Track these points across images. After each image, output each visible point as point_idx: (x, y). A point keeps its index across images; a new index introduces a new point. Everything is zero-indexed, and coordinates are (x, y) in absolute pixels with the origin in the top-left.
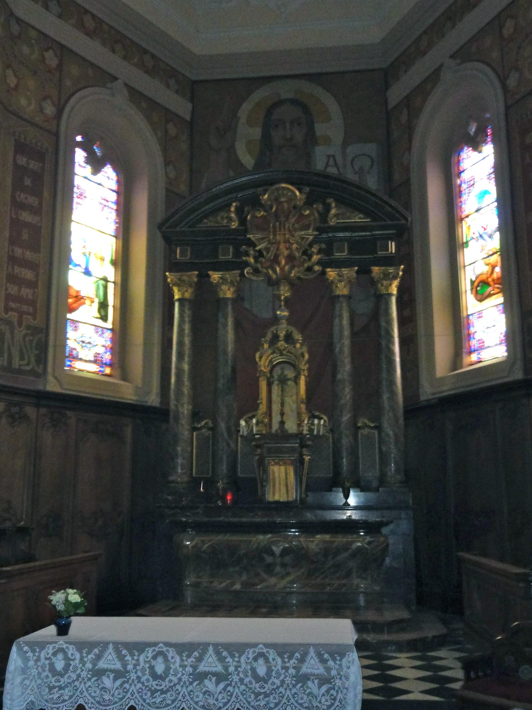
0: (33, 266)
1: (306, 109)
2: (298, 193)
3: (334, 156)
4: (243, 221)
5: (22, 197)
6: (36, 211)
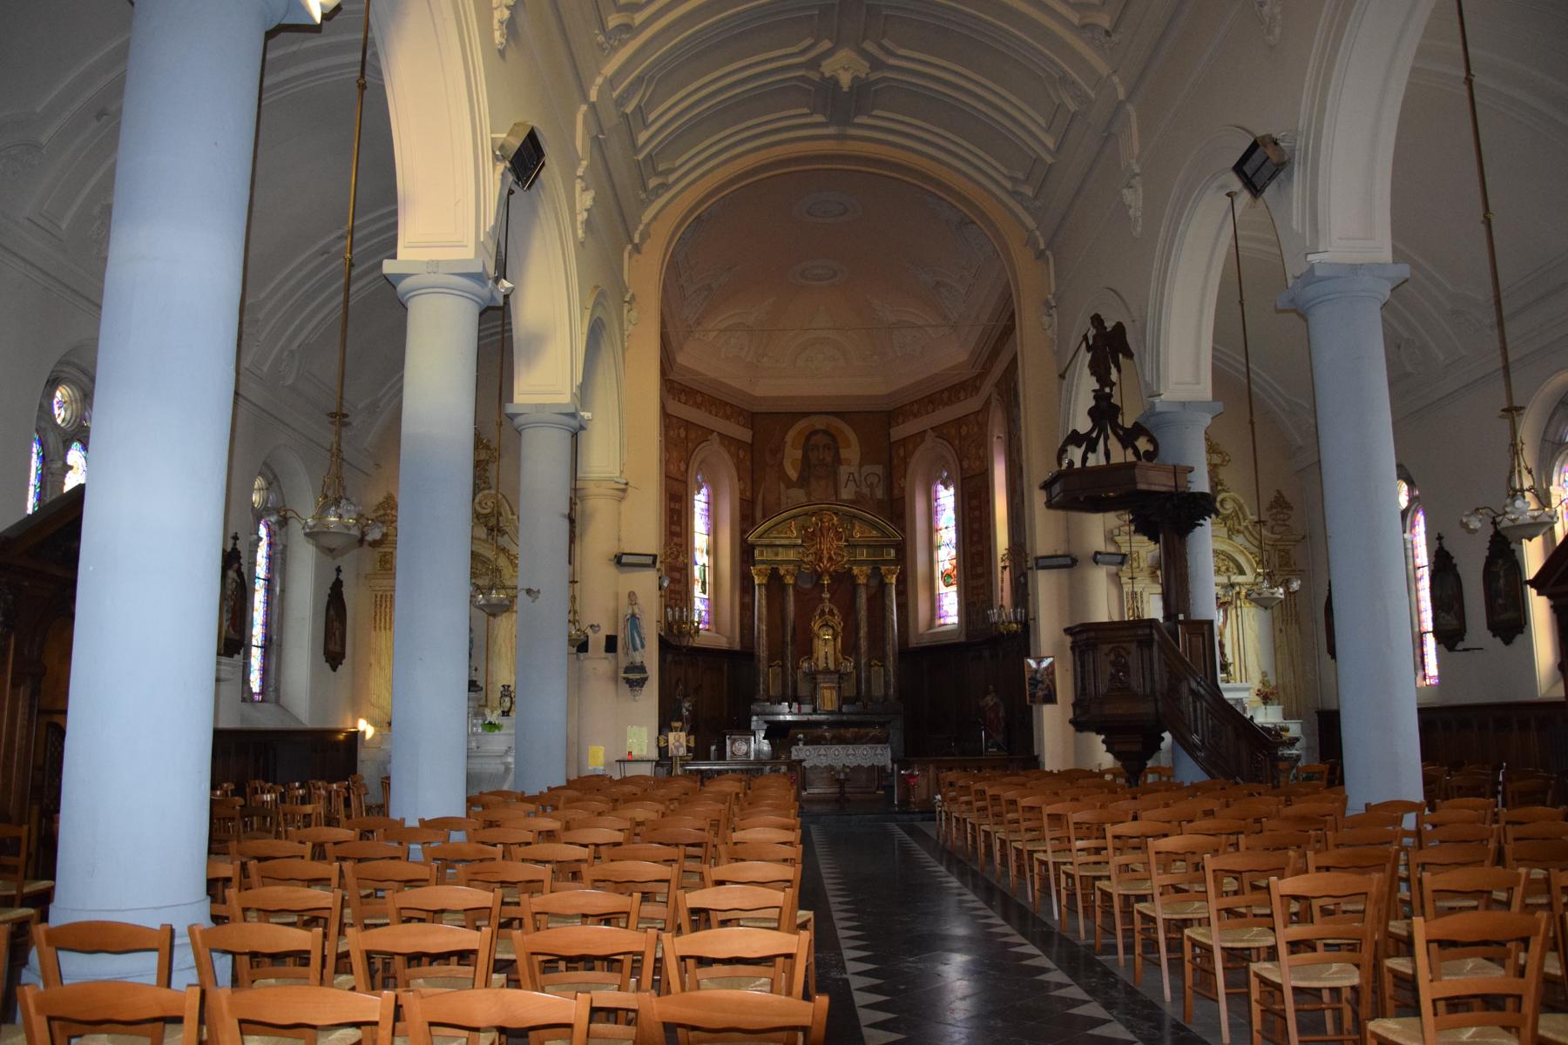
1: (833, 438)
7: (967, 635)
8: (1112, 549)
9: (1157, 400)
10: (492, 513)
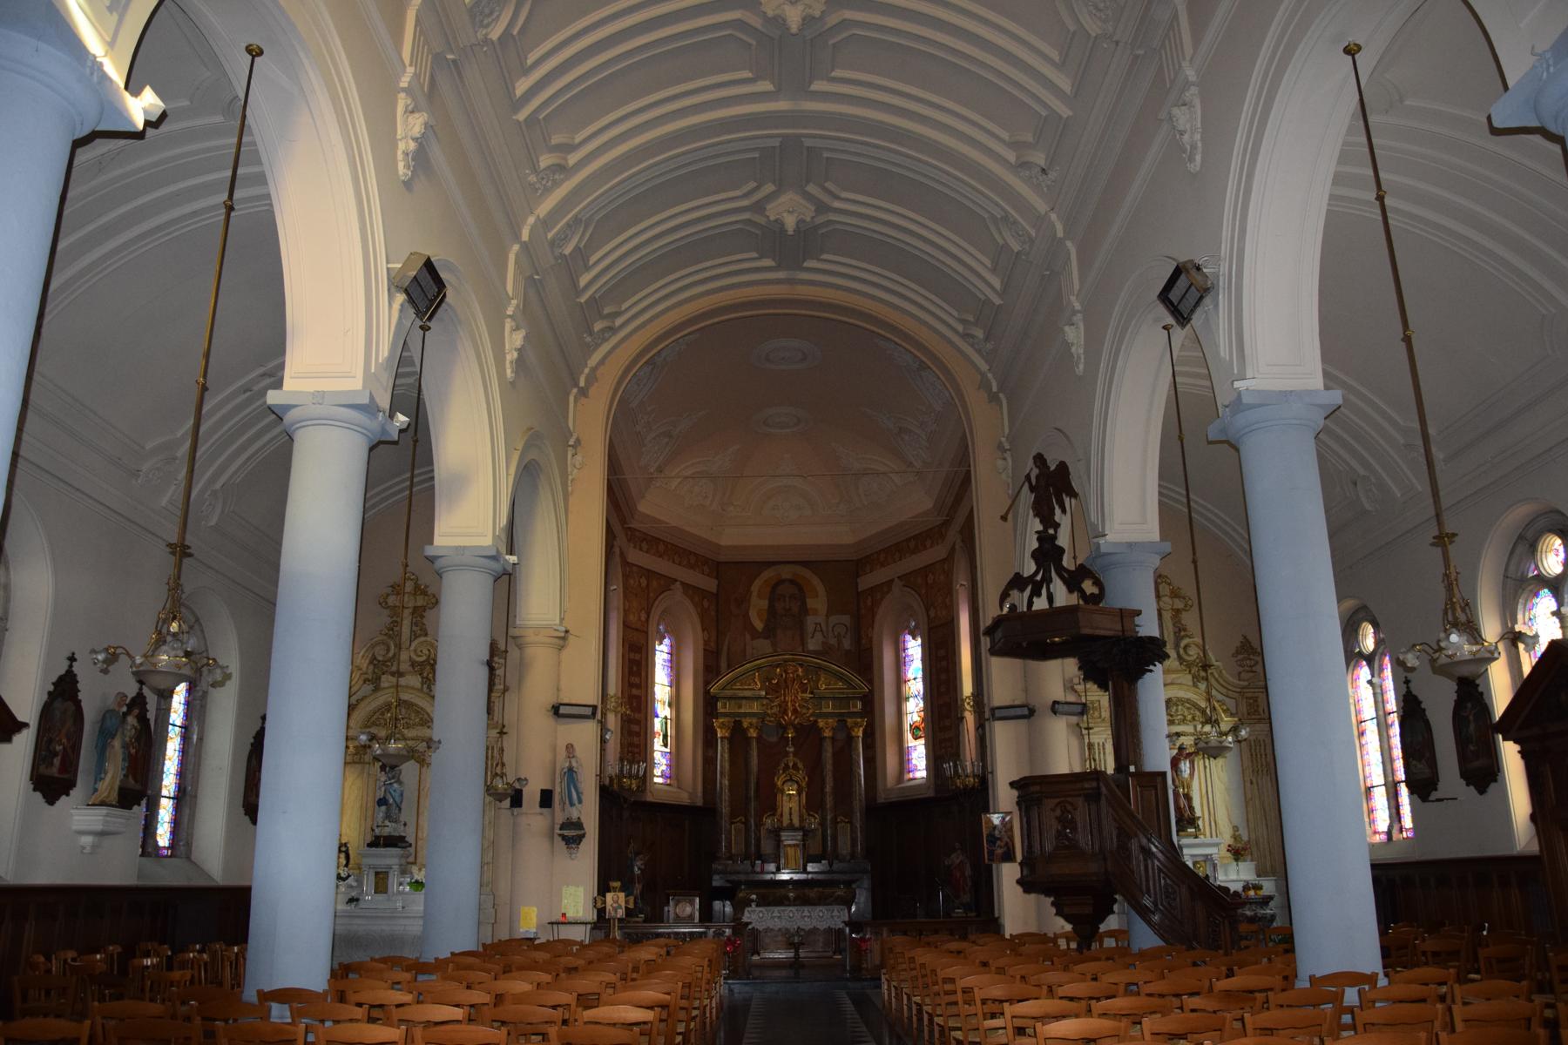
1: (801, 589)
8: (1071, 698)
9: (1102, 541)
10: (427, 660)
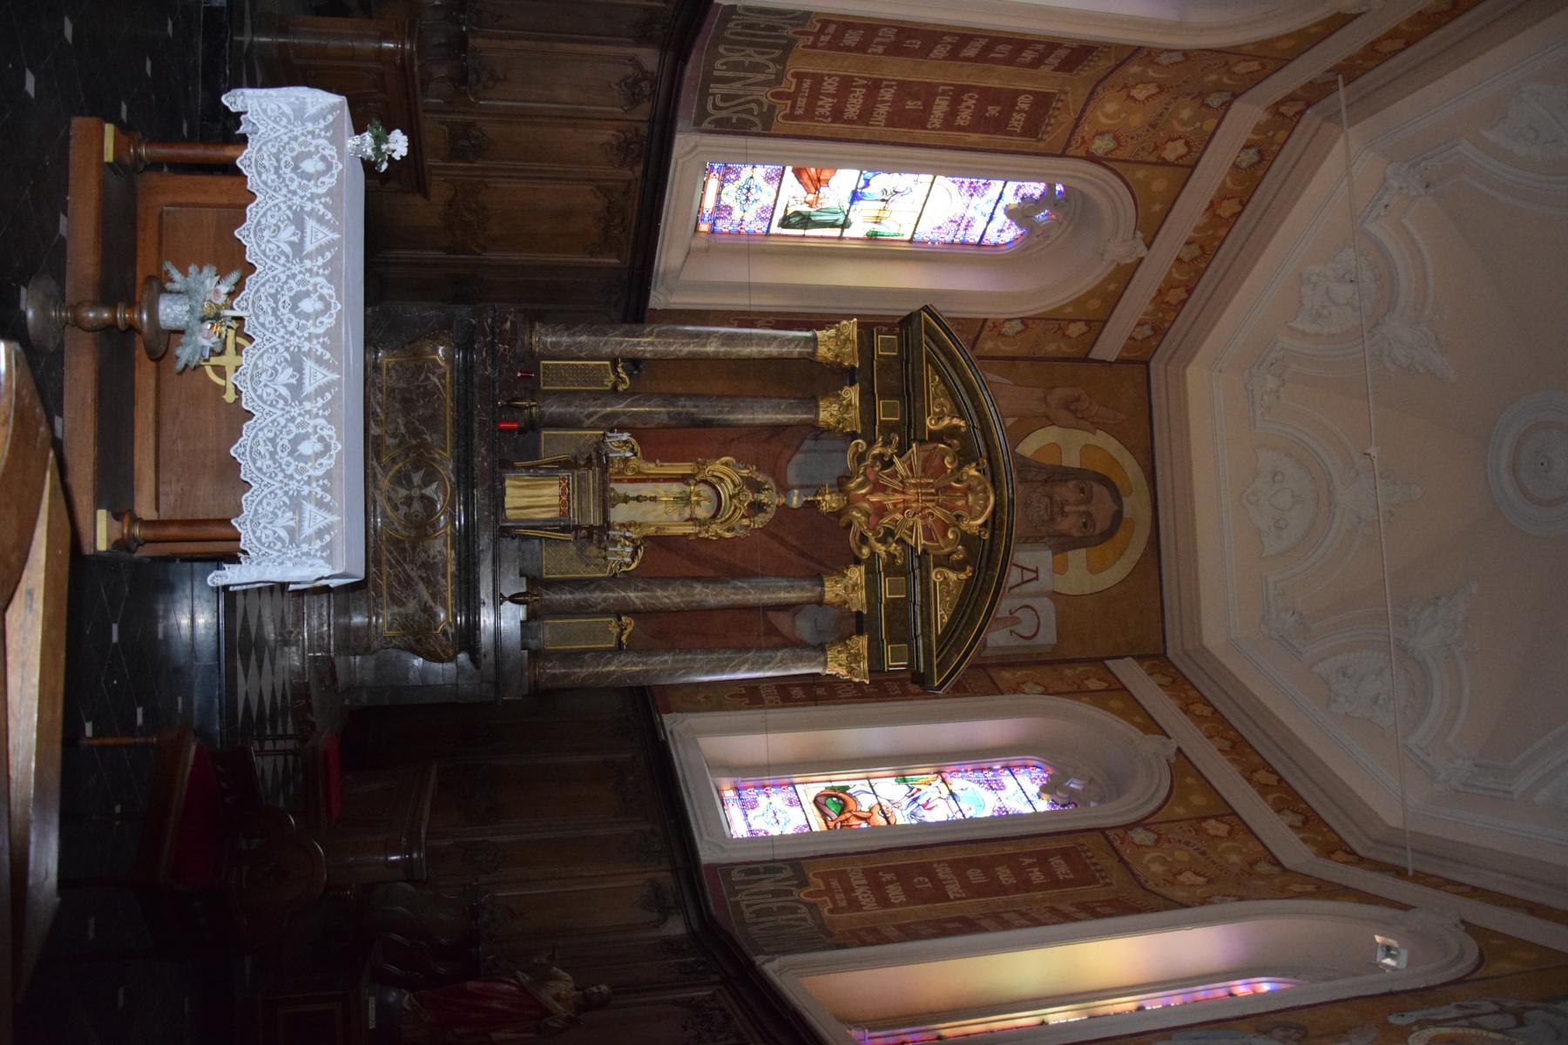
0: (865, 116)
1: (1108, 535)
2: (980, 521)
3: (1036, 578)
4: (937, 437)
5: (970, 101)
6: (949, 123)
7: (713, 867)
